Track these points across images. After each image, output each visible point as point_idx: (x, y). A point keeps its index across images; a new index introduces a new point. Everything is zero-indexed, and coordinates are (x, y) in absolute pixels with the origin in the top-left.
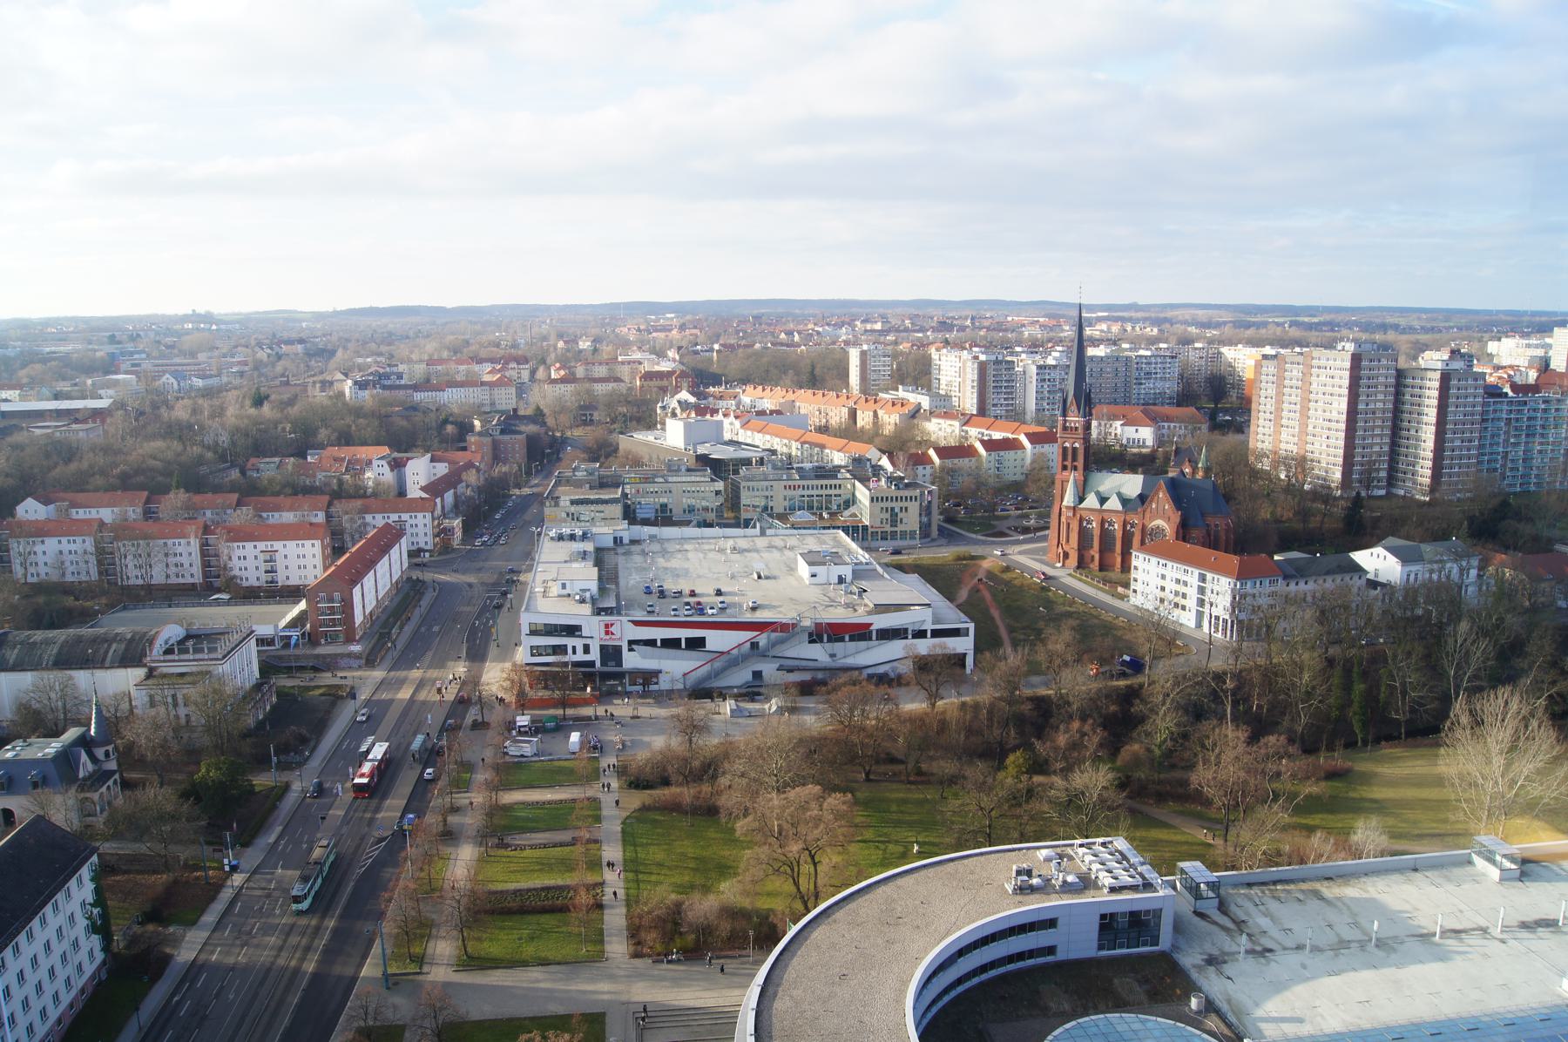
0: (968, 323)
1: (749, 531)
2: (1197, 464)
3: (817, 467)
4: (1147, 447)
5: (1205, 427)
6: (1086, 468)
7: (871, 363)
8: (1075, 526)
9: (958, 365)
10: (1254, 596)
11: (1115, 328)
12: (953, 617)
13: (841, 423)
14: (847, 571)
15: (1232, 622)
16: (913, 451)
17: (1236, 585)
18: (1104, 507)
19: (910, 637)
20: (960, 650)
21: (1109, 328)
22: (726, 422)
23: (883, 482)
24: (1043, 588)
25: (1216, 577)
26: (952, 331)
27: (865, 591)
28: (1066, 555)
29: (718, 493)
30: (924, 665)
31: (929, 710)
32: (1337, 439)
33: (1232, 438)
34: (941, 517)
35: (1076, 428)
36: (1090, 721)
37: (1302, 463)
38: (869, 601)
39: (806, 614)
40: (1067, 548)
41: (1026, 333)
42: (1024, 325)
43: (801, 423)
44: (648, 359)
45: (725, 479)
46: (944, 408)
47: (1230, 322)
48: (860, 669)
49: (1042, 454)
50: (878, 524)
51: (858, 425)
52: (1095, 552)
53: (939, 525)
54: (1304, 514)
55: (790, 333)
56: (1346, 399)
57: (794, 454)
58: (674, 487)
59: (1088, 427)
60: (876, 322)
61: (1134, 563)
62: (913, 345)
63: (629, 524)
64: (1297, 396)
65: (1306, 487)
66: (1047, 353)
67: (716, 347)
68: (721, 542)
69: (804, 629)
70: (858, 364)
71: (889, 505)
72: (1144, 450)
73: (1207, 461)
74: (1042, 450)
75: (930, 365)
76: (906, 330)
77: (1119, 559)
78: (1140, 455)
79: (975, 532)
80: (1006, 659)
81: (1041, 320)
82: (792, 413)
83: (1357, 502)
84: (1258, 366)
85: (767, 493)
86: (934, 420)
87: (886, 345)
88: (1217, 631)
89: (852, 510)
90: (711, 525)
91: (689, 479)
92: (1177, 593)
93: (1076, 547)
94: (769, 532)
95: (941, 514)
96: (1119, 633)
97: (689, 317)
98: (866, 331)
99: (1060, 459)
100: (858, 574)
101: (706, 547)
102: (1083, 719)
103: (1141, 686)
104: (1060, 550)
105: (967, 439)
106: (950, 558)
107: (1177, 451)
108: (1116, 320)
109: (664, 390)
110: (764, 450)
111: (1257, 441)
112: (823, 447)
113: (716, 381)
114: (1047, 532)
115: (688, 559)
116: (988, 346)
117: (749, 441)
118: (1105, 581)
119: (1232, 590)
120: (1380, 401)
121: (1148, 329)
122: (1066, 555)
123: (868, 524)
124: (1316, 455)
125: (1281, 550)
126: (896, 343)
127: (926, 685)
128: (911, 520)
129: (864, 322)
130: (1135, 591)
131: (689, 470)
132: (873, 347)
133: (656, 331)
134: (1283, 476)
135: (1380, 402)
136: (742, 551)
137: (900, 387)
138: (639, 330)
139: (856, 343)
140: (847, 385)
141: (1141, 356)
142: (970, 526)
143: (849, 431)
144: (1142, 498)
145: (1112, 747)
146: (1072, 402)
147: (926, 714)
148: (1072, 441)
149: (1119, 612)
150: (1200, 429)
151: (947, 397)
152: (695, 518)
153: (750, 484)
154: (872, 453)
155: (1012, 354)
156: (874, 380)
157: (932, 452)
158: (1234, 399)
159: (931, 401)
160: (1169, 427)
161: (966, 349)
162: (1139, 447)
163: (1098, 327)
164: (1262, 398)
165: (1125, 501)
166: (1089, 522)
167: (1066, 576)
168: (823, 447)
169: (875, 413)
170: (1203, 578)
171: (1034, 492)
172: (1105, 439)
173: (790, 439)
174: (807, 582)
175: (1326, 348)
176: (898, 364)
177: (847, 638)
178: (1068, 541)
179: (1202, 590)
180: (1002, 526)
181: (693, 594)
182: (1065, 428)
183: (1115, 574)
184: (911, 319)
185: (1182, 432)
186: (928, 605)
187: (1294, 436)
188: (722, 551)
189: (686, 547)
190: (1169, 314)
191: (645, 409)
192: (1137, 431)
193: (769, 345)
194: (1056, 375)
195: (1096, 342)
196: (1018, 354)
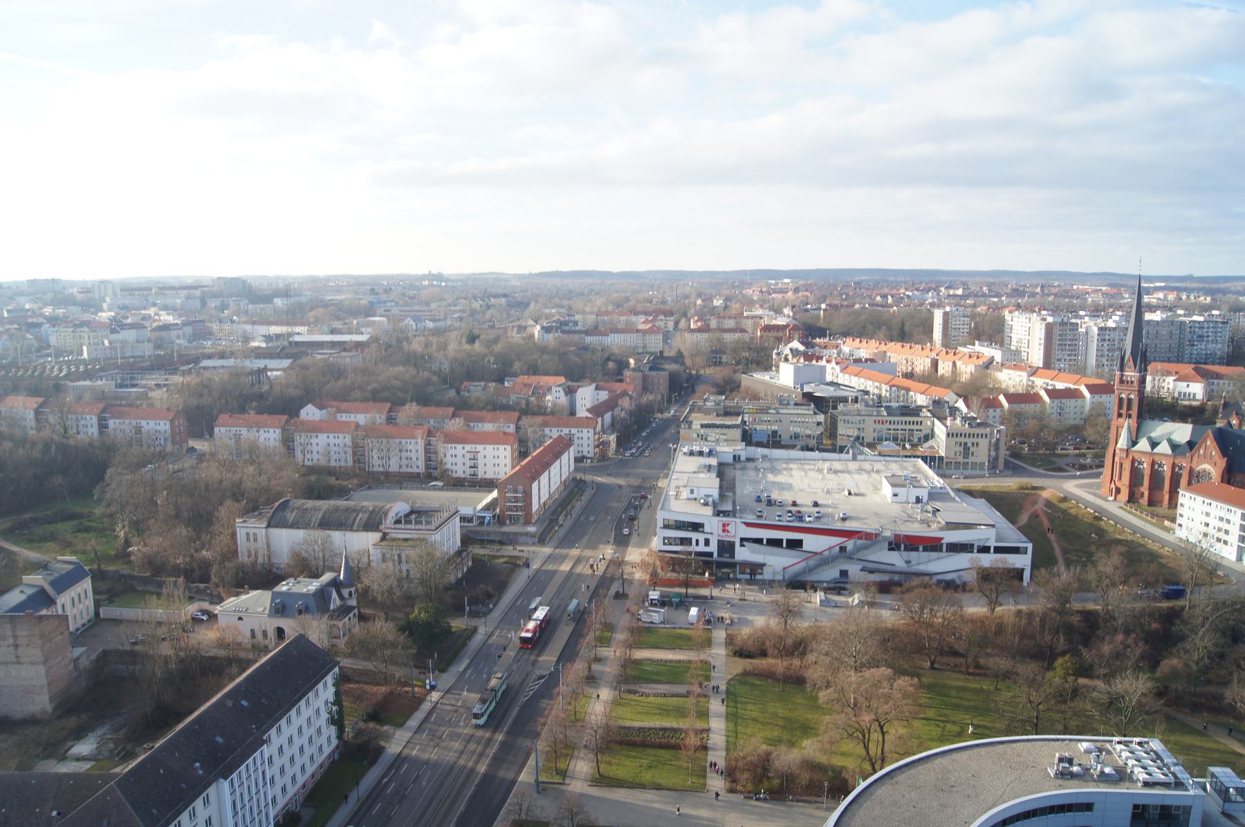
0: (1038, 290)
1: (843, 456)
3: (905, 407)
4: (1197, 400)
6: (1140, 416)
7: (953, 323)
9: (1028, 325)
11: (1171, 297)
12: (1014, 537)
13: (924, 370)
14: (924, 494)
16: (986, 396)
18: (1156, 450)
19: (975, 551)
20: (1019, 565)
21: (1165, 297)
22: (829, 367)
23: (958, 421)
24: (1096, 518)
27: (938, 510)
29: (819, 424)
30: (986, 576)
31: (989, 614)
34: (1008, 453)
35: (1132, 382)
36: (1133, 635)
38: (942, 519)
39: (888, 527)
41: (1090, 300)
42: (1088, 293)
43: (891, 369)
44: (768, 315)
45: (825, 413)
46: (1015, 360)
48: (931, 575)
49: (1100, 403)
50: (952, 455)
51: (939, 373)
52: (1145, 489)
53: (1005, 459)
55: (884, 296)
57: (883, 394)
58: (783, 418)
59: (1142, 381)
60: (958, 288)
61: (1181, 500)
62: (989, 308)
63: (746, 445)
66: (1108, 317)
67: (823, 306)
68: (820, 464)
69: (885, 538)
71: (963, 440)
72: (1194, 403)
74: (1100, 400)
75: (1003, 325)
76: (984, 295)
77: (1166, 497)
78: (1190, 407)
79: (1038, 467)
80: (1059, 575)
81: (1104, 288)
82: (883, 361)
85: (859, 426)
86: (1005, 371)
89: (931, 443)
90: (812, 450)
91: (796, 412)
92: (1220, 530)
94: (859, 457)
95: (1007, 450)
96: (1164, 561)
97: (802, 282)
98: (949, 296)
99: (1116, 408)
100: (934, 495)
101: (807, 467)
102: (1127, 632)
103: (1183, 608)
105: (1033, 388)
106: (1014, 487)
107: (1226, 405)
108: (1172, 289)
109: (779, 340)
110: (859, 391)
112: (908, 390)
113: (822, 333)
114: (1101, 470)
115: (792, 476)
116: (1055, 310)
117: (847, 383)
118: (1153, 515)
121: (1202, 298)
122: (1118, 491)
123: (943, 455)
126: (974, 306)
127: (988, 593)
128: (982, 453)
130: (1180, 525)
131: (796, 404)
132: (954, 309)
133: (775, 292)
136: (836, 472)
137: (977, 342)
138: (761, 292)
140: (931, 340)
141: (1194, 322)
142: (1033, 460)
143: (931, 378)
144: (1191, 445)
145: (1152, 662)
146: (1129, 360)
147: (987, 617)
148: (1127, 392)
149: (1164, 543)
151: (1017, 352)
152: (799, 444)
153: (846, 418)
154: (949, 396)
155: (1077, 317)
156: (955, 336)
157: (1001, 398)
159: (1003, 355)
160: (1218, 384)
161: (1034, 311)
162: (1190, 400)
163: (1155, 296)
165: (1174, 446)
166: (1140, 463)
167: (1115, 507)
168: (908, 390)
169: (954, 363)
171: (1091, 434)
173: (881, 383)
174: (890, 501)
176: (976, 324)
178: (1120, 478)
180: (1061, 462)
181: (794, 504)
182: (1122, 381)
183: (1163, 509)
185: (1231, 388)
186: (993, 526)
188: (820, 471)
189: (792, 466)
190: (1222, 286)
191: (763, 354)
192: (1188, 386)
193: (867, 306)
194: (1115, 335)
195: (1152, 308)
196: (1082, 317)
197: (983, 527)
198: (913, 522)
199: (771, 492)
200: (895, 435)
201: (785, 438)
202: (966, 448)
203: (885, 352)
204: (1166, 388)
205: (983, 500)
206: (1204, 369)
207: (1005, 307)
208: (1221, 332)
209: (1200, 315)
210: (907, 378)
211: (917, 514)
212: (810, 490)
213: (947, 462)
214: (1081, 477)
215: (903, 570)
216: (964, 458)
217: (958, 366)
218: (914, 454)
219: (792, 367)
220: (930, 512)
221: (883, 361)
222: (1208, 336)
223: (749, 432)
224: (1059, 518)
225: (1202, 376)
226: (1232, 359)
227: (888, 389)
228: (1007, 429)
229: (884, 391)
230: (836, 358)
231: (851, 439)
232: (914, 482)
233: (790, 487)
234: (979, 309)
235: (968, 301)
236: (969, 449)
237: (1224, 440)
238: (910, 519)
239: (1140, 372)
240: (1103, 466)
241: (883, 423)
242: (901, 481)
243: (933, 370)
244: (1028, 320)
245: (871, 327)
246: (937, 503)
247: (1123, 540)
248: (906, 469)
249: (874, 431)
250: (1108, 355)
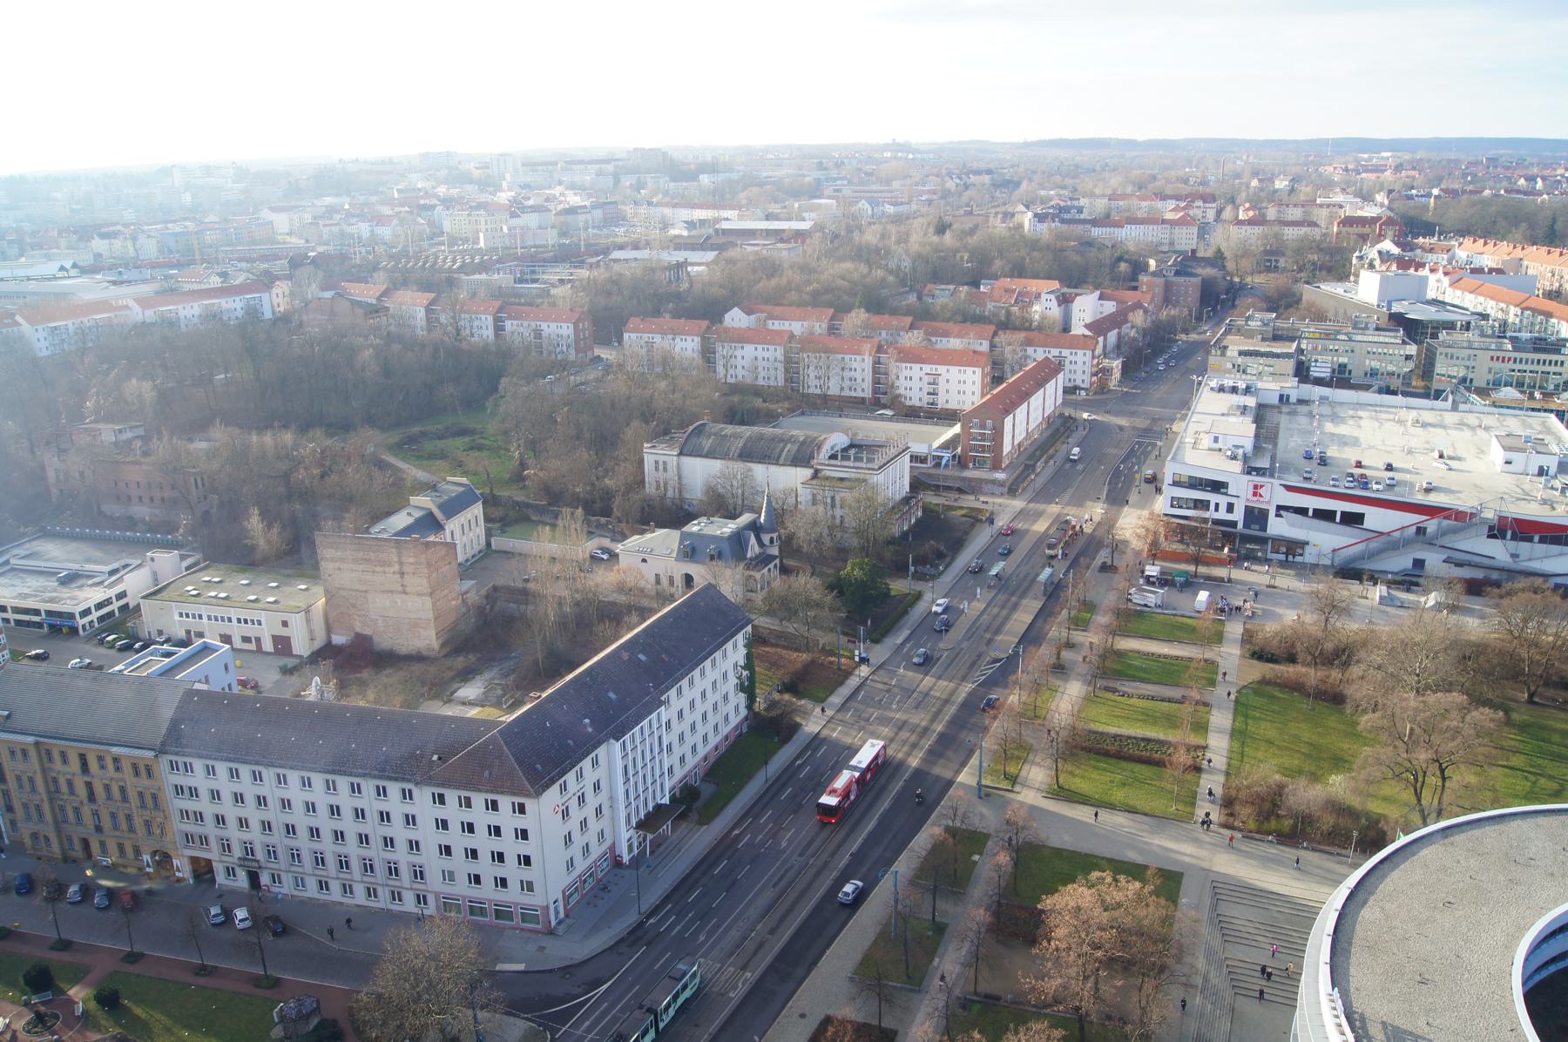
1: (1438, 404)
3: (1536, 338)
22: (1432, 278)
29: (1408, 358)
39: (1491, 505)
43: (1529, 284)
44: (1351, 203)
48: (1546, 576)
55: (1531, 179)
57: (1510, 320)
58: (1357, 347)
63: (1299, 382)
68: (1403, 413)
82: (1516, 273)
85: (1468, 363)
90: (1394, 393)
94: (1462, 407)
97: (1407, 156)
101: (1384, 416)
109: (1364, 238)
110: (1473, 314)
112: (1549, 315)
113: (1428, 230)
115: (1360, 427)
131: (1377, 329)
133: (1367, 171)
136: (1425, 425)
138: (1346, 170)
152: (1376, 383)
153: (1449, 350)
168: (1549, 315)
173: (1508, 303)
174: (1499, 469)
177: (1536, 538)
181: (1359, 465)
188: (1401, 422)
189: (1361, 413)
193: (1502, 192)
198: (1529, 501)
200: (1521, 380)
203: (1521, 259)
210: (1550, 299)
211: (1538, 491)
212: (1383, 448)
215: (1507, 566)
218: (1546, 407)
220: (1557, 490)
221: (1516, 273)
223: (1306, 365)
227: (1519, 313)
229: (1513, 314)
230: (1444, 266)
231: (1454, 381)
232: (1539, 446)
233: (1355, 442)
238: (1526, 497)
242: (1520, 443)
245: (1504, 223)
248: (1531, 427)
249: (1490, 372)
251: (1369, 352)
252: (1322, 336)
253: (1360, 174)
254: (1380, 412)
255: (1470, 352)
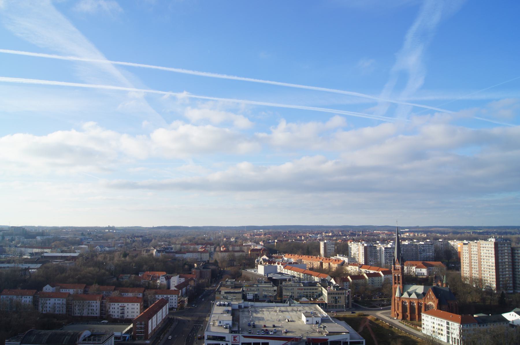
1: (285, 304)
2: (443, 281)
3: (309, 282)
4: (425, 276)
5: (445, 268)
6: (404, 284)
7: (328, 247)
8: (400, 304)
10: (468, 330)
11: (411, 235)
13: (317, 267)
14: (319, 320)
15: (460, 340)
16: (342, 277)
17: (460, 326)
18: (410, 297)
22: (278, 266)
23: (332, 288)
24: (390, 327)
25: (453, 323)
26: (356, 236)
27: (326, 327)
28: (398, 315)
29: (275, 291)
32: (493, 272)
33: (455, 272)
34: (353, 300)
35: (399, 269)
37: (480, 281)
39: (304, 335)
40: (398, 312)
42: (380, 234)
44: (253, 245)
45: (277, 286)
46: (353, 262)
47: (452, 232)
49: (388, 278)
50: (330, 303)
51: (323, 268)
52: (408, 313)
53: (352, 303)
54: (483, 300)
55: (301, 237)
56: (494, 258)
57: (301, 277)
59: (402, 269)
60: (330, 233)
61: (423, 318)
62: (342, 241)
63: (244, 301)
64: (476, 257)
65: (483, 290)
66: (388, 243)
67: (276, 241)
70: (323, 247)
71: (334, 296)
72: (424, 277)
73: (446, 281)
74: (387, 277)
76: (340, 236)
77: (417, 316)
78: (423, 278)
81: (386, 232)
83: (503, 295)
84: (462, 247)
85: (292, 291)
86: (350, 266)
87: (333, 240)
88: (455, 342)
89: (321, 297)
90: (272, 302)
91: (265, 286)
92: (439, 329)
93: (401, 312)
94: (292, 305)
95: (353, 299)
97: (267, 231)
98: (326, 236)
99: (393, 280)
100: (324, 320)
101: (270, 310)
104: (396, 313)
105: (361, 273)
106: (356, 315)
107: (436, 277)
108: (411, 232)
109: (258, 255)
110: (291, 276)
111: (464, 273)
114: (390, 306)
115: (264, 314)
116: (367, 241)
117: (286, 273)
118: (413, 324)
119: (460, 328)
120: (506, 259)
121: (423, 235)
122: (398, 315)
123: (327, 302)
124: (486, 278)
125: (475, 314)
126: (336, 240)
128: (342, 301)
129: (326, 233)
130: (424, 328)
131: (265, 282)
133: (256, 235)
134: (474, 286)
135: (507, 259)
136: (282, 312)
137: (338, 255)
138: (251, 235)
139: (322, 240)
140: (320, 254)
143: (320, 270)
144: (424, 294)
146: (396, 260)
148: (397, 273)
149: (418, 336)
150: (443, 269)
151: (354, 258)
152: (267, 299)
153: (286, 288)
154: (328, 277)
156: (329, 253)
157: (349, 277)
158: (455, 258)
159: (348, 260)
160: (432, 269)
161: (360, 242)
162: (422, 276)
163: (405, 234)
164: (464, 258)
165: (418, 295)
166: (405, 303)
167: (397, 322)
168: (311, 275)
169: (329, 264)
170: (448, 324)
171: (385, 291)
172: (410, 273)
173: (300, 272)
174: (305, 323)
175: (485, 241)
178: (398, 309)
179: (448, 328)
181: (265, 326)
182: (395, 269)
183: (416, 322)
184: (341, 232)
187: (477, 271)
188: (276, 311)
189: (264, 309)
192: (421, 270)
193: (294, 240)
194: (390, 251)
195: (404, 239)
196: (378, 244)
197: (344, 333)
198: (315, 332)
199: (255, 321)
201: (261, 298)
202: (336, 300)
203: (301, 259)
204: (412, 271)
205: (344, 321)
206: (426, 263)
207: (349, 240)
208: (431, 248)
209: (423, 242)
210: (311, 270)
211: (317, 329)
212: (271, 320)
213: (328, 306)
214: (383, 310)
216: (335, 303)
217: (331, 265)
218: (315, 302)
219: (263, 266)
220: (322, 328)
221: (301, 263)
222: (426, 250)
224: (375, 327)
225: (426, 266)
226: (437, 258)
227: (303, 275)
228: (352, 290)
231: (289, 297)
233: (262, 319)
234: (338, 241)
235: (334, 238)
236: (337, 299)
237: (436, 291)
238: (314, 331)
239: (401, 265)
240: (391, 305)
241: (301, 290)
243: (321, 267)
244: (357, 245)
246: (325, 324)
247: (402, 336)
249: (298, 293)
250: (389, 259)
251: (263, 290)
252: (249, 286)
253: (255, 236)
254: (269, 308)
255: (291, 288)
